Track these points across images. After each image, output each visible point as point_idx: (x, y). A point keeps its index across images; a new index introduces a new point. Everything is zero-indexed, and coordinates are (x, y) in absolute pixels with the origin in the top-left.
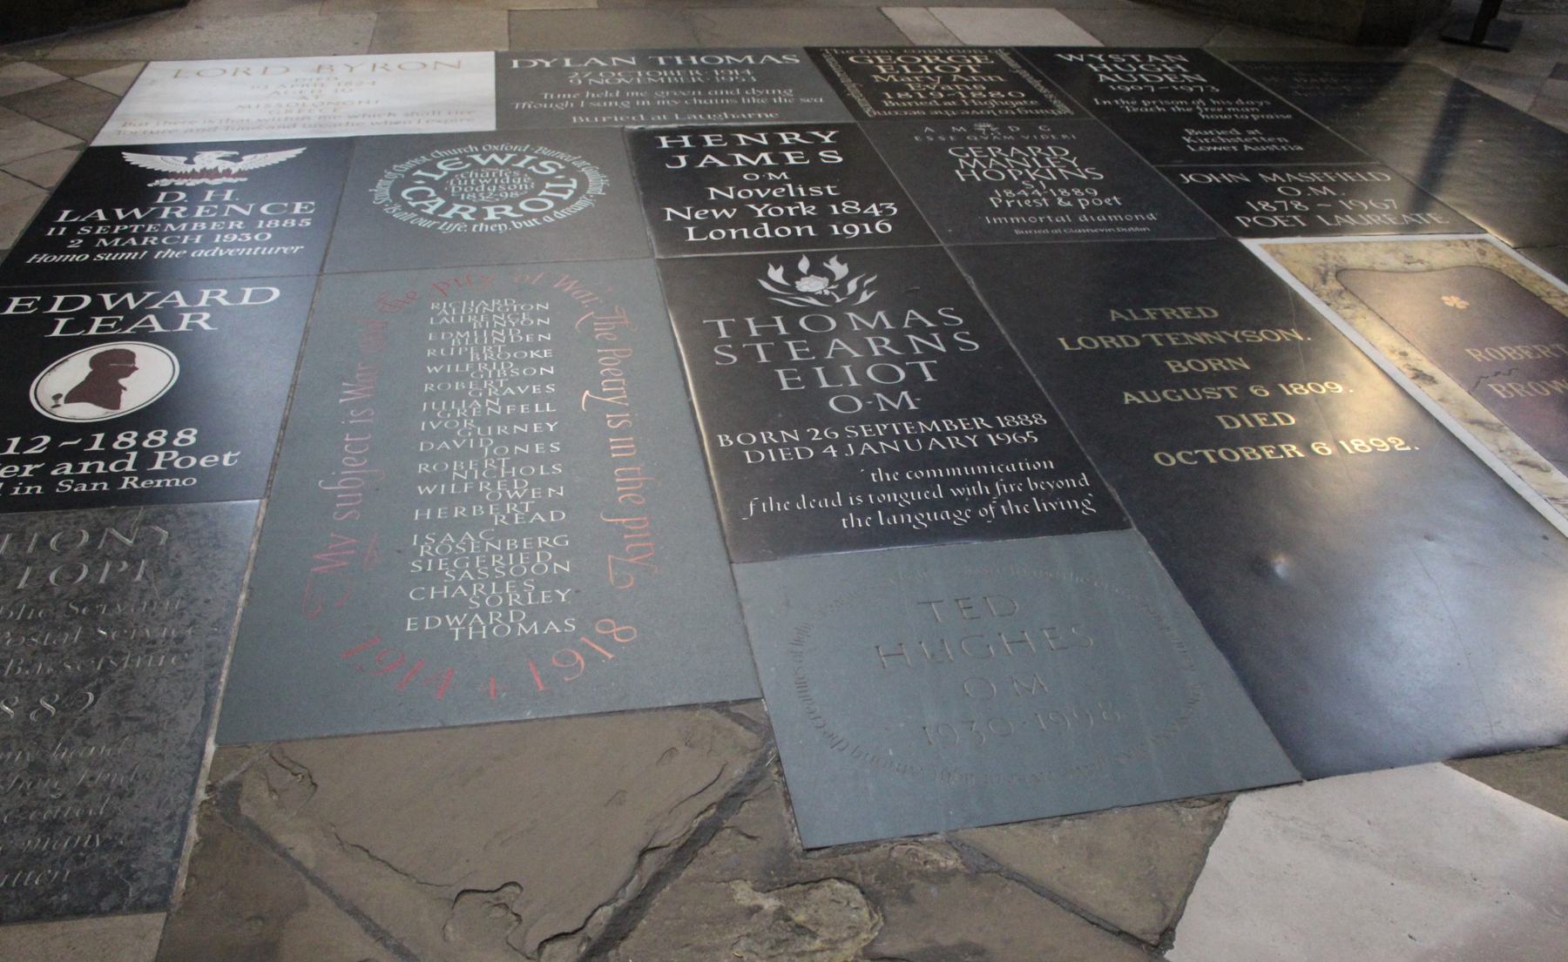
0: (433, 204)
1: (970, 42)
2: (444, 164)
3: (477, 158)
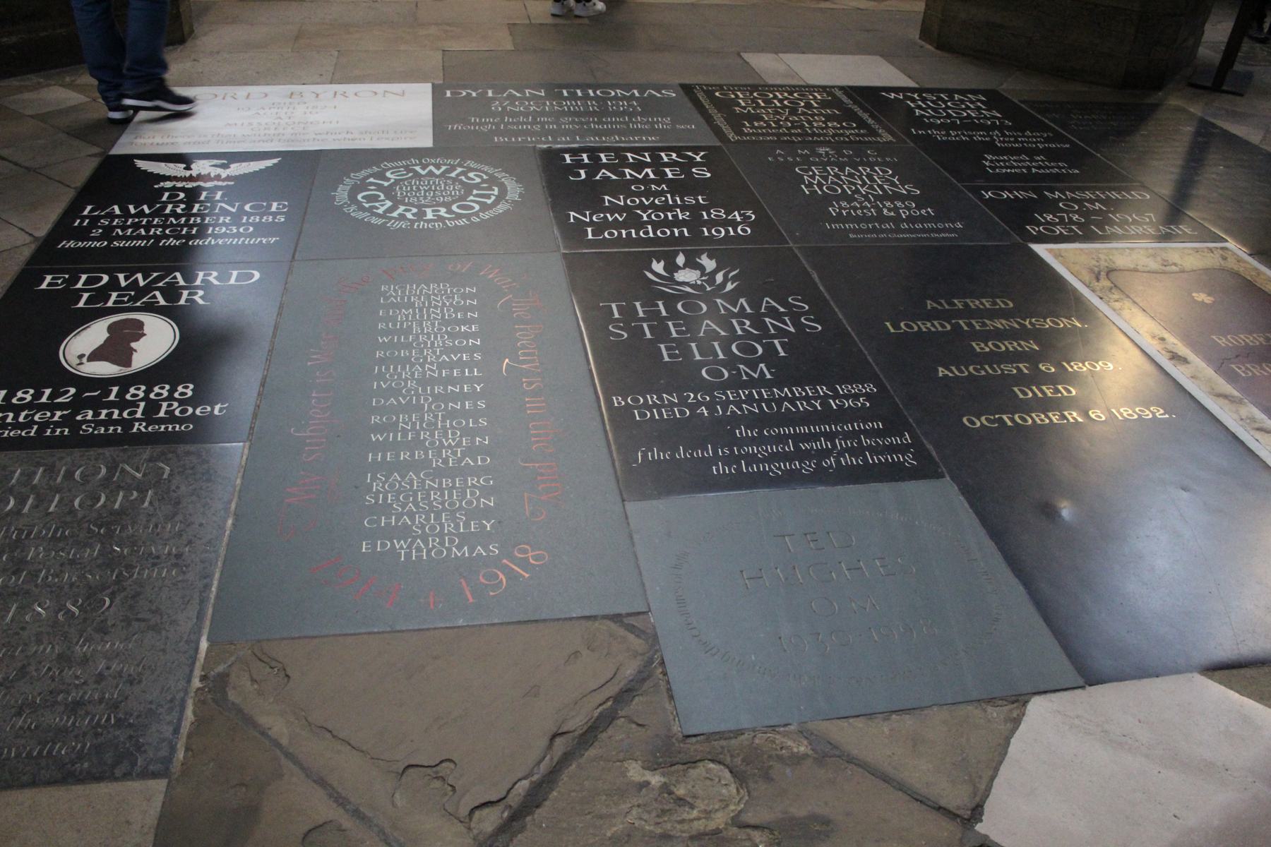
0: (382, 205)
1: (811, 82)
2: (392, 173)
3: (418, 168)
